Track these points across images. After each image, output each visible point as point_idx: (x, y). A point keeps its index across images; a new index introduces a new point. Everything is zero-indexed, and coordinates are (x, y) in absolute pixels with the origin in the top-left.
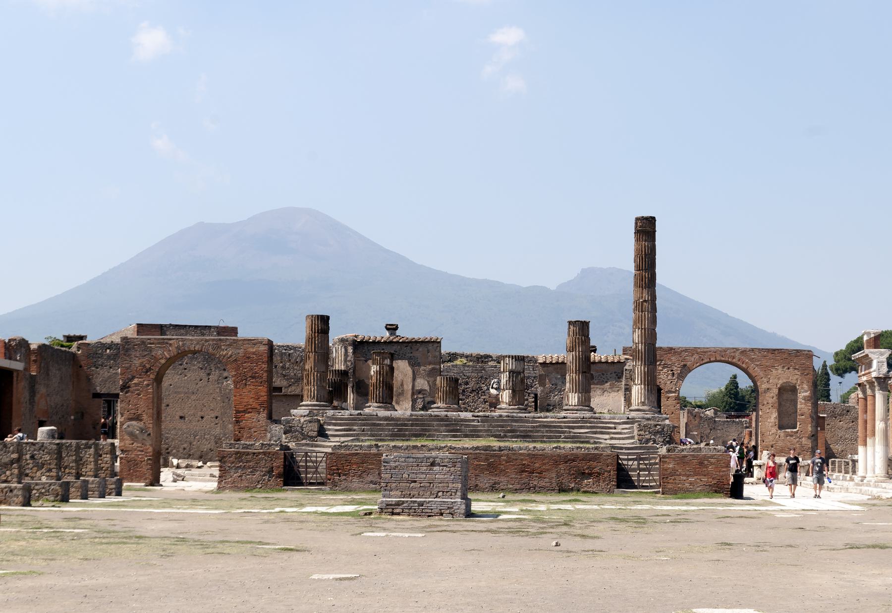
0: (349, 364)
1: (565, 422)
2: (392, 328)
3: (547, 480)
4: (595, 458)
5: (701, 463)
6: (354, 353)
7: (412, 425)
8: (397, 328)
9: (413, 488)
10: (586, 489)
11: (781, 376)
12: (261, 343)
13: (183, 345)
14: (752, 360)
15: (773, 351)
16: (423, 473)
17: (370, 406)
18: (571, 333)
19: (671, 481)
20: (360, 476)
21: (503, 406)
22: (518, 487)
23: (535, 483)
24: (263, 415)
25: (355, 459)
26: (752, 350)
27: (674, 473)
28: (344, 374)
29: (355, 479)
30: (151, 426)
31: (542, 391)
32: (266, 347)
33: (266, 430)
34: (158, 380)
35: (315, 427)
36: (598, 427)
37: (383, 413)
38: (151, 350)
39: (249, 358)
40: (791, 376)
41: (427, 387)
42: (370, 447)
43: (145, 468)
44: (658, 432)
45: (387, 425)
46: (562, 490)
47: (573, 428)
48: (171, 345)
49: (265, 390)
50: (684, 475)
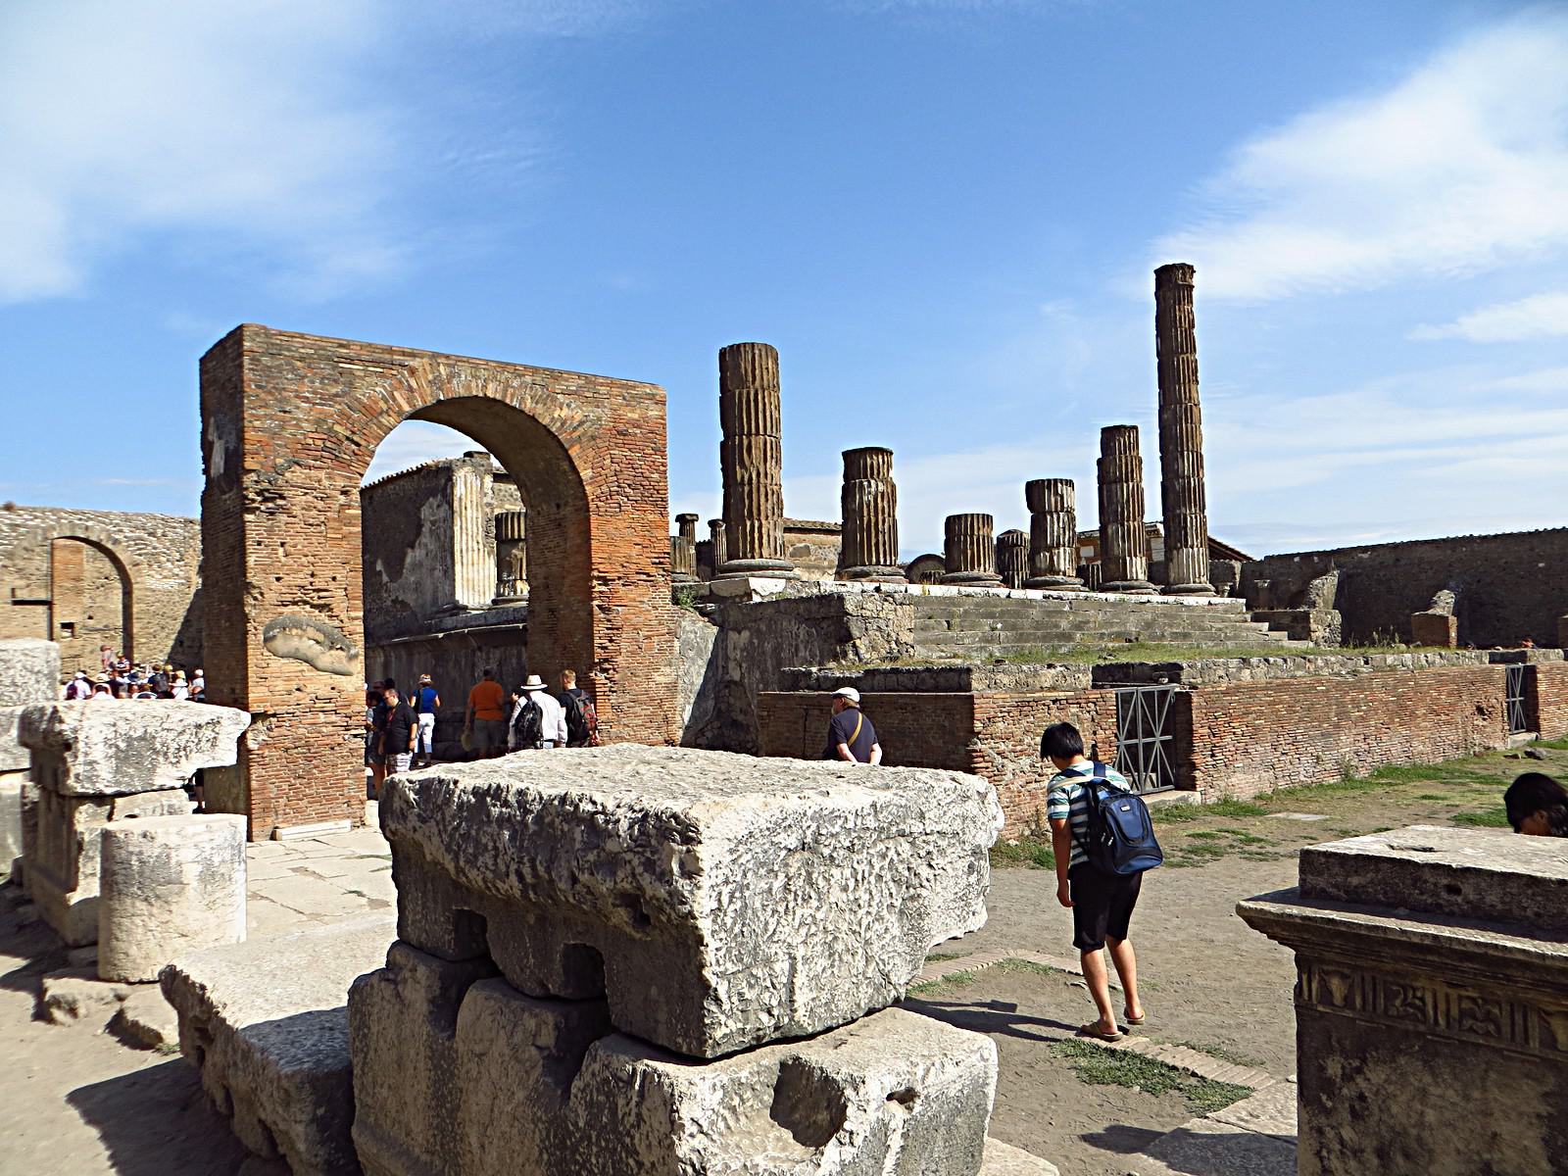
13: (451, 376)
21: (1059, 578)
48: (413, 372)
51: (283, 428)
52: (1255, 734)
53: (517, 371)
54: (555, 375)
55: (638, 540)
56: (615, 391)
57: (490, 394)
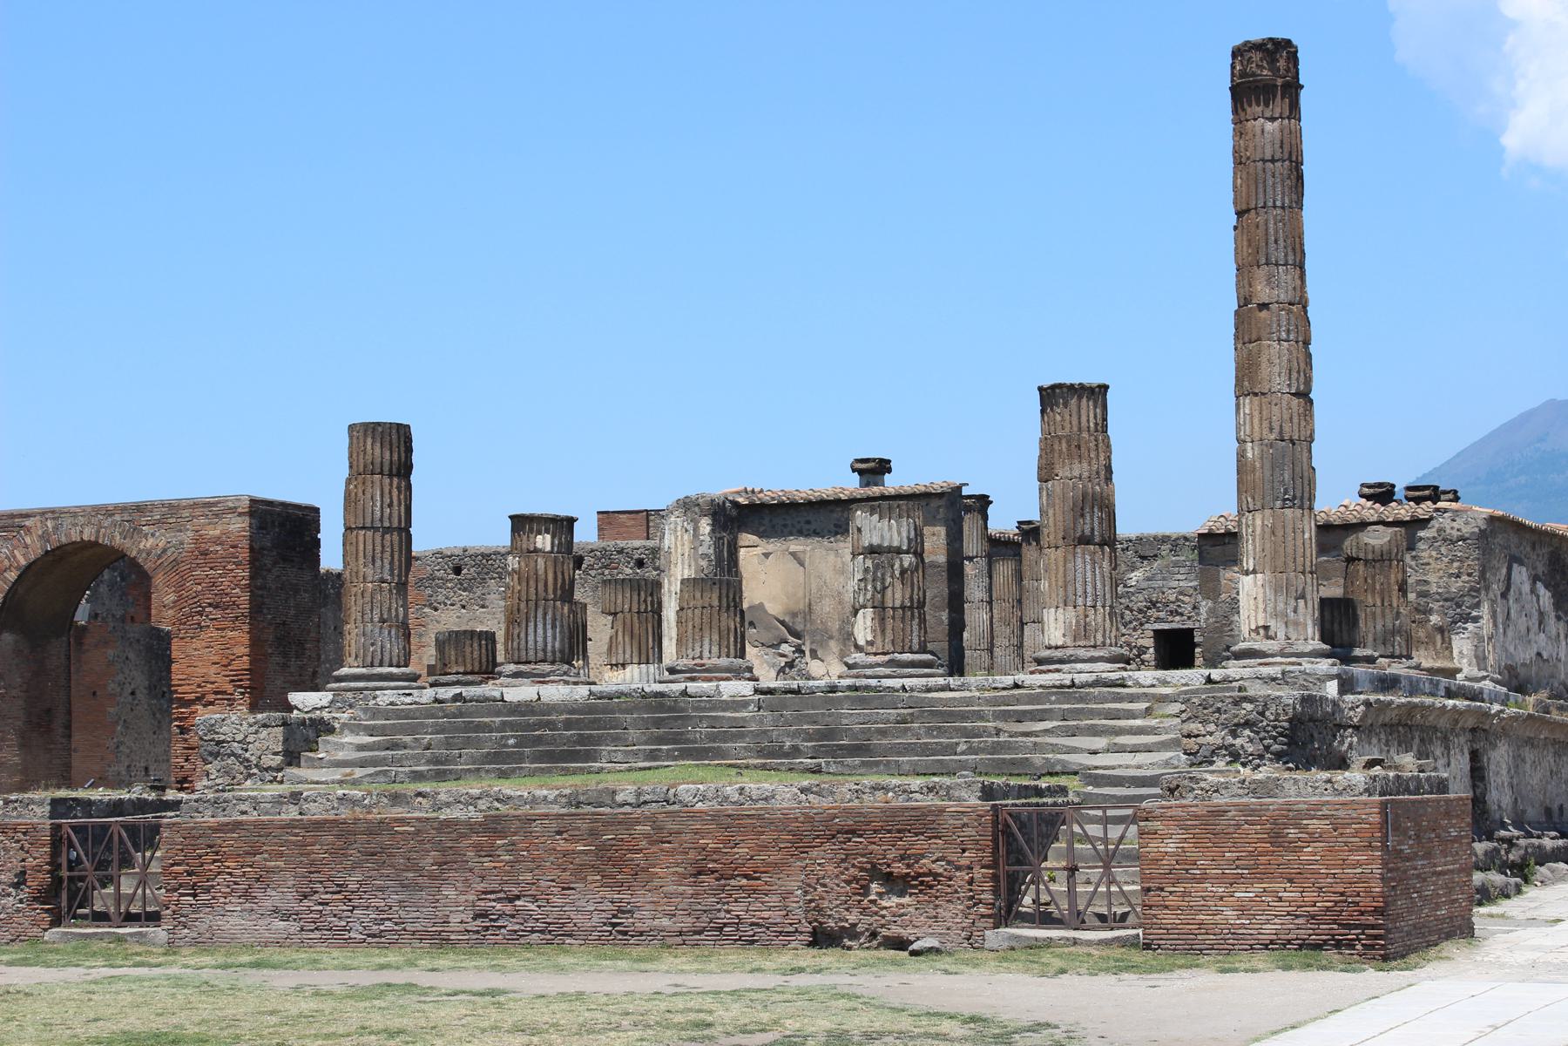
0: (704, 563)
2: (873, 469)
3: (773, 900)
4: (922, 823)
5: (1276, 838)
7: (568, 725)
8: (883, 466)
10: (895, 930)
12: (233, 510)
13: (56, 528)
19: (1172, 901)
20: (247, 895)
22: (687, 923)
23: (738, 909)
25: (230, 842)
27: (1183, 870)
29: (234, 904)
31: (1211, 611)
36: (1092, 714)
39: (205, 553)
42: (279, 801)
44: (1248, 724)
46: (823, 938)
47: (1020, 717)
48: (28, 530)
49: (246, 638)
50: (1220, 879)
53: (107, 511)
54: (140, 508)
55: (216, 659)
57: (86, 538)
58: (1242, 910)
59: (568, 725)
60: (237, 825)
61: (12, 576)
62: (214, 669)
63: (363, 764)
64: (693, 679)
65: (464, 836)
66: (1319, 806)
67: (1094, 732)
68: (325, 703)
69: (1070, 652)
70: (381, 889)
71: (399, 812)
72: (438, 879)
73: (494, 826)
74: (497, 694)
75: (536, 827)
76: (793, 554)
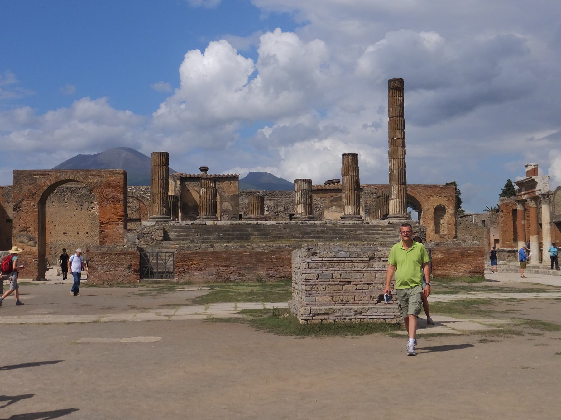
0: (178, 192)
1: (344, 227)
2: (204, 169)
5: (462, 255)
6: (181, 185)
7: (233, 231)
9: (346, 291)
11: (436, 200)
12: (119, 173)
13: (60, 175)
14: (418, 192)
15: (430, 186)
16: (359, 272)
17: (200, 218)
18: (345, 163)
19: (440, 268)
24: (121, 226)
26: (418, 185)
28: (176, 197)
30: (37, 236)
32: (122, 176)
33: (123, 237)
34: (42, 203)
35: (161, 233)
37: (210, 223)
38: (36, 179)
39: (110, 184)
40: (442, 201)
41: (230, 208)
43: (34, 268)
45: (215, 231)
48: (51, 176)
50: (449, 264)
51: (21, 192)
52: (206, 266)
56: (107, 173)
57: (70, 178)
58: (455, 270)
59: (233, 231)
60: (197, 253)
61: (46, 188)
62: (112, 215)
63: (183, 240)
64: (257, 220)
65: (263, 255)
66: (472, 248)
67: (373, 234)
68: (153, 224)
69: (353, 216)
70: (240, 268)
71: (242, 249)
72: (256, 266)
73: (272, 253)
74: (204, 223)
75: (283, 253)
76: (196, 191)
